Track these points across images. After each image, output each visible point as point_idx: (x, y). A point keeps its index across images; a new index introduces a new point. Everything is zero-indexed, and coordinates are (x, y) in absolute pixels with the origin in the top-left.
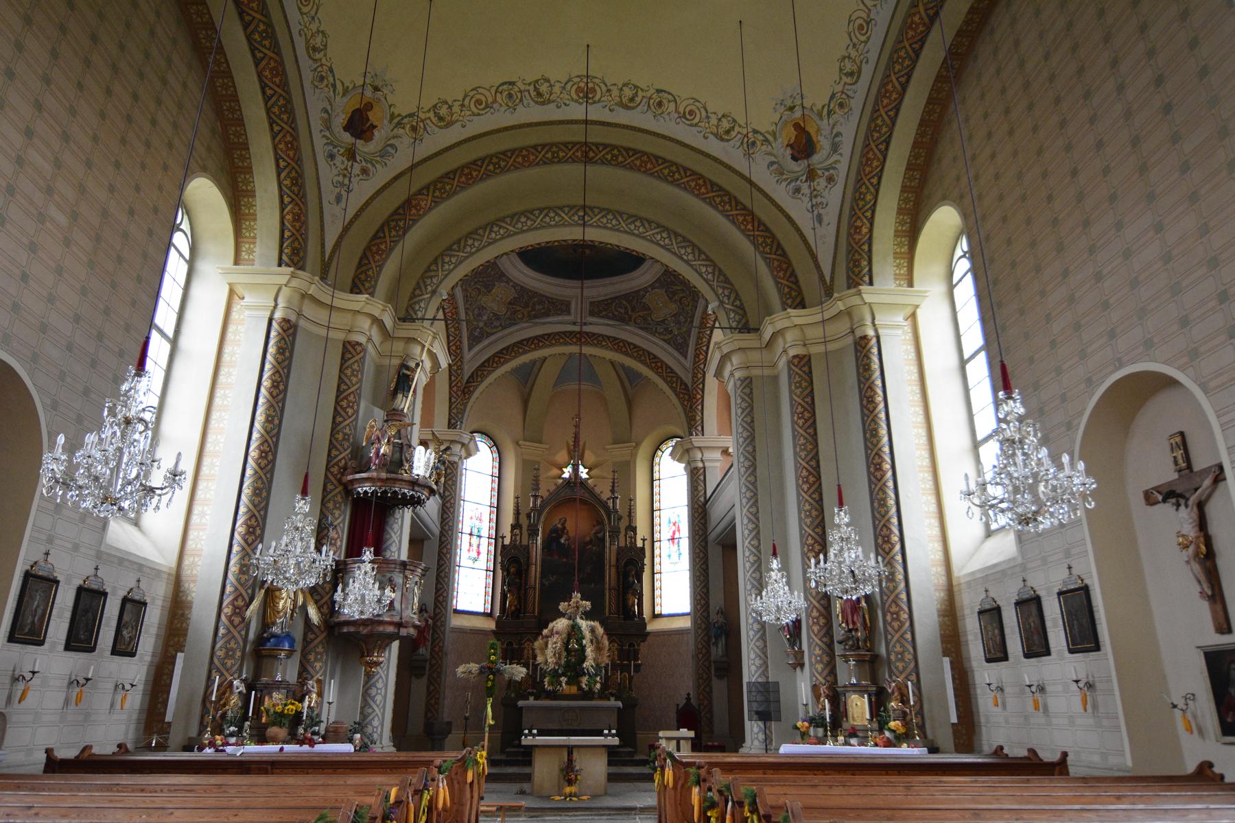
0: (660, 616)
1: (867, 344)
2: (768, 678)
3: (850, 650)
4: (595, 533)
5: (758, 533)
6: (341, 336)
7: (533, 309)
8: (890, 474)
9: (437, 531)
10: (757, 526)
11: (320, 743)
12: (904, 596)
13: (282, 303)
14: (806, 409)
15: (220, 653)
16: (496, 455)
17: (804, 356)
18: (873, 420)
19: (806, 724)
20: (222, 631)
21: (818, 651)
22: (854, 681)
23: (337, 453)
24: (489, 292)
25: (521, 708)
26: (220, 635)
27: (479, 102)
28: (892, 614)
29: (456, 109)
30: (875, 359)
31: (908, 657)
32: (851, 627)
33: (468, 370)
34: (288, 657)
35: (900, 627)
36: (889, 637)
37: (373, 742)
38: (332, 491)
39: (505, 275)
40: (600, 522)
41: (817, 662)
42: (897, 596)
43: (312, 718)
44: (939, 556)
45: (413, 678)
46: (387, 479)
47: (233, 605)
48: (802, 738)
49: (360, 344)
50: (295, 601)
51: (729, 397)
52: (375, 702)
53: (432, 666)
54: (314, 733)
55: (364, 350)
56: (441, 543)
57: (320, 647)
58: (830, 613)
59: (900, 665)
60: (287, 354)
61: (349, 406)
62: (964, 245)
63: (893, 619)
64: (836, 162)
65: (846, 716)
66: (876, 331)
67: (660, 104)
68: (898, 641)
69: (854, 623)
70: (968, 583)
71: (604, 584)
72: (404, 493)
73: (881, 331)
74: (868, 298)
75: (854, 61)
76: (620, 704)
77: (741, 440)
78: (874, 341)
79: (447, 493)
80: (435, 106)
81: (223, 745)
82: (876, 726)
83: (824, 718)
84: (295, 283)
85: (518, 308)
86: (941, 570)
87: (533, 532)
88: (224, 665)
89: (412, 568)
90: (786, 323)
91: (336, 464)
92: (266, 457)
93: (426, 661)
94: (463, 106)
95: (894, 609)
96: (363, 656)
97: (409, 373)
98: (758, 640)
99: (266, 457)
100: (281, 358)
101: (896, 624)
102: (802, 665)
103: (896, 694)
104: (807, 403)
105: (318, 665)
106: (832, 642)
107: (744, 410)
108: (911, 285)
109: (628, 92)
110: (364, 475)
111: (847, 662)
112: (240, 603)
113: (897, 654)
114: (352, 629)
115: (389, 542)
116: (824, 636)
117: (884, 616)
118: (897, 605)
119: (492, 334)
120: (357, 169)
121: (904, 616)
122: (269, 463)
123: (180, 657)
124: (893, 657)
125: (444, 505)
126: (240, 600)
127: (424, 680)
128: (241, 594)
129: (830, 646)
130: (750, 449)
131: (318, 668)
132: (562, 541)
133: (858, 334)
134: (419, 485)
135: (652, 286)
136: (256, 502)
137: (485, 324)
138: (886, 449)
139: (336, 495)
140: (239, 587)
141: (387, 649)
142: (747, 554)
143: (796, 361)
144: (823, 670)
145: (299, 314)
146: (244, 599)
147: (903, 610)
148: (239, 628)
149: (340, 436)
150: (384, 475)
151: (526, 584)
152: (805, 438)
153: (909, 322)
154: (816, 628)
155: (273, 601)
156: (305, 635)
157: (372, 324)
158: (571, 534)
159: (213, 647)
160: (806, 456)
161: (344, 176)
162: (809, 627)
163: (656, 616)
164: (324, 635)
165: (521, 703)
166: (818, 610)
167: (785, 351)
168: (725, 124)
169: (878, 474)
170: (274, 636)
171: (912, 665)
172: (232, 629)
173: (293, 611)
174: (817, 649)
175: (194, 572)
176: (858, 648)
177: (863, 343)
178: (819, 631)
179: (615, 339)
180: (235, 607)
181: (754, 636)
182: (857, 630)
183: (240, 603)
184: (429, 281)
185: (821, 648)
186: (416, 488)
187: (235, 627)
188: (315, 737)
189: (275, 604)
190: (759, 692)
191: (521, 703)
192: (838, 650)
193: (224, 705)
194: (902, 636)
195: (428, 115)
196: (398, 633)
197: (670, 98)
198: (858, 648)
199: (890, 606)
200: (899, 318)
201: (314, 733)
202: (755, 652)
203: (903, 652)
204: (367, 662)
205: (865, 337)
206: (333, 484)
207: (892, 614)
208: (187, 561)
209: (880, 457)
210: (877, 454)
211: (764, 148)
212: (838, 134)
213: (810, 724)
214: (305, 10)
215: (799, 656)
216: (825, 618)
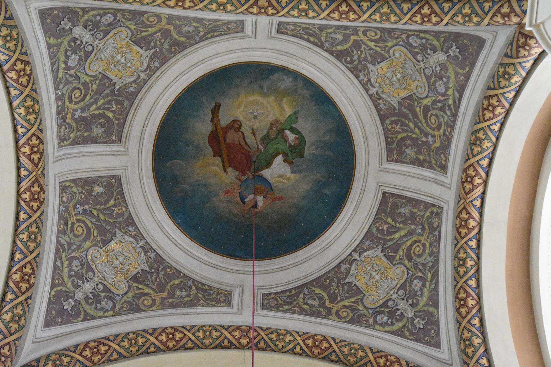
7: (171, 295)
24: (106, 243)
39: (133, 224)
85: (147, 290)
119: (93, 318)
135: (360, 249)
137: (87, 298)
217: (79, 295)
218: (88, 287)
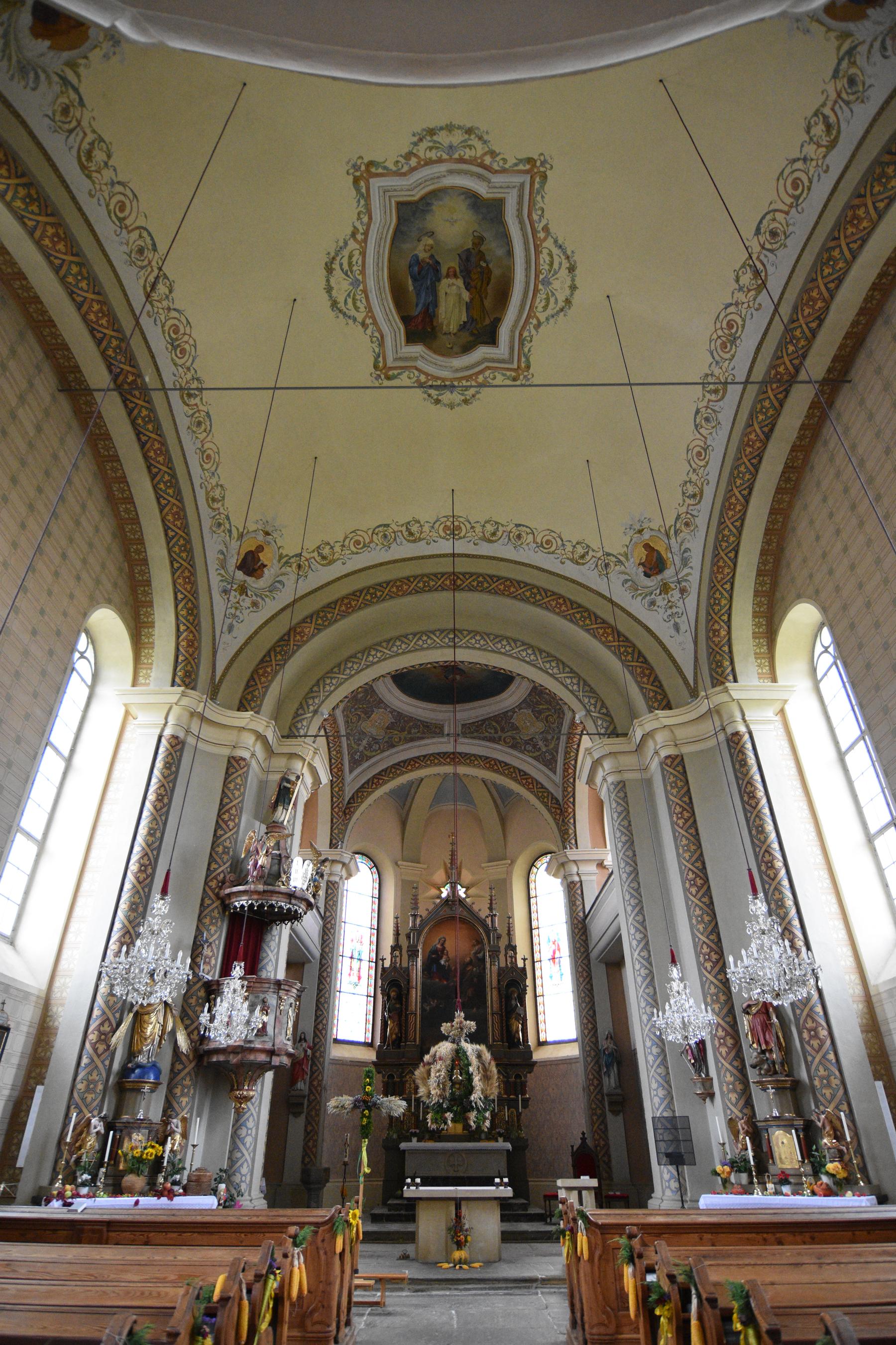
0: (545, 1043)
1: (740, 740)
2: (674, 1111)
3: (766, 1075)
4: (476, 953)
5: (647, 943)
6: (226, 752)
8: (783, 872)
9: (317, 953)
10: (645, 936)
11: (180, 1195)
12: (819, 1009)
13: (172, 720)
14: (684, 809)
15: (80, 1086)
16: (376, 876)
17: (677, 756)
18: (757, 816)
19: (727, 1168)
20: (85, 1060)
21: (729, 1078)
22: (776, 1113)
23: (216, 866)
25: (404, 1151)
26: (83, 1065)
27: (357, 543)
28: (809, 1031)
29: (337, 548)
30: (751, 754)
31: (835, 1082)
32: (764, 1047)
33: (348, 793)
34: (152, 1091)
35: (821, 1046)
36: (809, 1058)
37: (240, 1194)
38: (209, 905)
40: (479, 942)
41: (729, 1091)
42: (811, 1009)
43: (173, 1165)
44: (850, 961)
45: (291, 1117)
46: (264, 891)
47: (99, 1031)
48: (725, 1187)
49: (244, 759)
50: (164, 1026)
51: (601, 803)
52: (244, 1144)
53: (310, 1103)
54: (175, 1183)
55: (248, 765)
56: (322, 965)
57: (188, 1079)
58: (737, 1032)
59: (827, 1092)
60: (174, 769)
61: (230, 819)
62: (826, 636)
63: (811, 1037)
64: (687, 575)
65: (772, 1158)
66: (747, 726)
67: (519, 537)
68: (820, 1063)
69: (767, 1043)
70: (890, 992)
71: (486, 1007)
72: (281, 907)
73: (752, 727)
74: (735, 695)
75: (696, 484)
76: (509, 1146)
77: (620, 845)
78: (747, 737)
79: (328, 914)
80: (319, 547)
81: (72, 1197)
82: (808, 1169)
83: (746, 1161)
84: (185, 701)
86: (855, 978)
87: (413, 954)
88: (83, 1099)
89: (287, 988)
90: (655, 725)
91: (215, 878)
92: (145, 871)
93: (304, 1097)
94: (343, 546)
95: (810, 1024)
96: (232, 1090)
97: (288, 785)
98: (658, 1066)
99: (145, 871)
100: (167, 772)
101: (815, 1043)
102: (712, 1096)
103: (828, 1128)
104: (685, 802)
105: (184, 1100)
106: (744, 1066)
107: (620, 814)
108: (774, 680)
109: (490, 528)
110: (241, 888)
111: (765, 1089)
112: (106, 1028)
113: (822, 1078)
114: (221, 1058)
115: (265, 961)
116: (734, 1059)
117: (800, 1034)
118: (814, 1020)
119: (371, 757)
120: (247, 602)
121: (824, 1033)
122: (148, 877)
123: (40, 1089)
124: (817, 1083)
125: (324, 926)
126: (106, 1024)
127: (301, 1120)
128: (108, 1019)
129: (742, 1070)
130: (630, 853)
131: (184, 1104)
132: (442, 962)
133: (729, 731)
134: (296, 898)
135: (519, 707)
136: (132, 918)
138: (776, 846)
139: (213, 910)
140: (107, 1010)
141: (259, 1082)
142: (637, 967)
143: (669, 761)
144: (738, 1100)
145: (188, 732)
146: (110, 1024)
147: (821, 1025)
148: (103, 1057)
149: (220, 849)
150: (261, 887)
151: (407, 1009)
152: (687, 839)
153: (778, 718)
154: (724, 1050)
155: (141, 1026)
156: (173, 1065)
157: (257, 740)
158: (452, 954)
159: (74, 1080)
160: (691, 857)
161: (236, 608)
162: (716, 1050)
163: (541, 1044)
164: (193, 1065)
165: (403, 1145)
166: (724, 1029)
167: (656, 753)
168: (580, 550)
169: (771, 873)
170: (139, 1066)
171: (841, 1092)
172: (96, 1058)
173: (161, 1037)
174: (728, 1075)
175: (64, 994)
176: (776, 1073)
177: (735, 739)
178: (728, 1054)
179: (487, 758)
180: (101, 1033)
181: (655, 1061)
182: (771, 1051)
183: (106, 1028)
184: (311, 702)
185: (732, 1074)
186: (293, 901)
187: (99, 1056)
188: (176, 1188)
189: (142, 1030)
190: (666, 1129)
191: (403, 1145)
192: (753, 1075)
193: (80, 1148)
194: (824, 1057)
195: (312, 555)
196: (270, 1062)
197: (528, 530)
198: (776, 1073)
199: (805, 1021)
200: (770, 713)
201: (175, 1183)
202: (657, 1081)
203: (829, 1076)
204: (236, 1097)
205: (737, 734)
206: (210, 898)
207: (809, 1031)
208: (57, 983)
209: (770, 854)
210: (766, 851)
211: (618, 568)
212: (687, 550)
213: (732, 1167)
214: (206, 466)
215: (708, 1084)
216: (732, 1037)
217: (361, 748)
218: (364, 742)
